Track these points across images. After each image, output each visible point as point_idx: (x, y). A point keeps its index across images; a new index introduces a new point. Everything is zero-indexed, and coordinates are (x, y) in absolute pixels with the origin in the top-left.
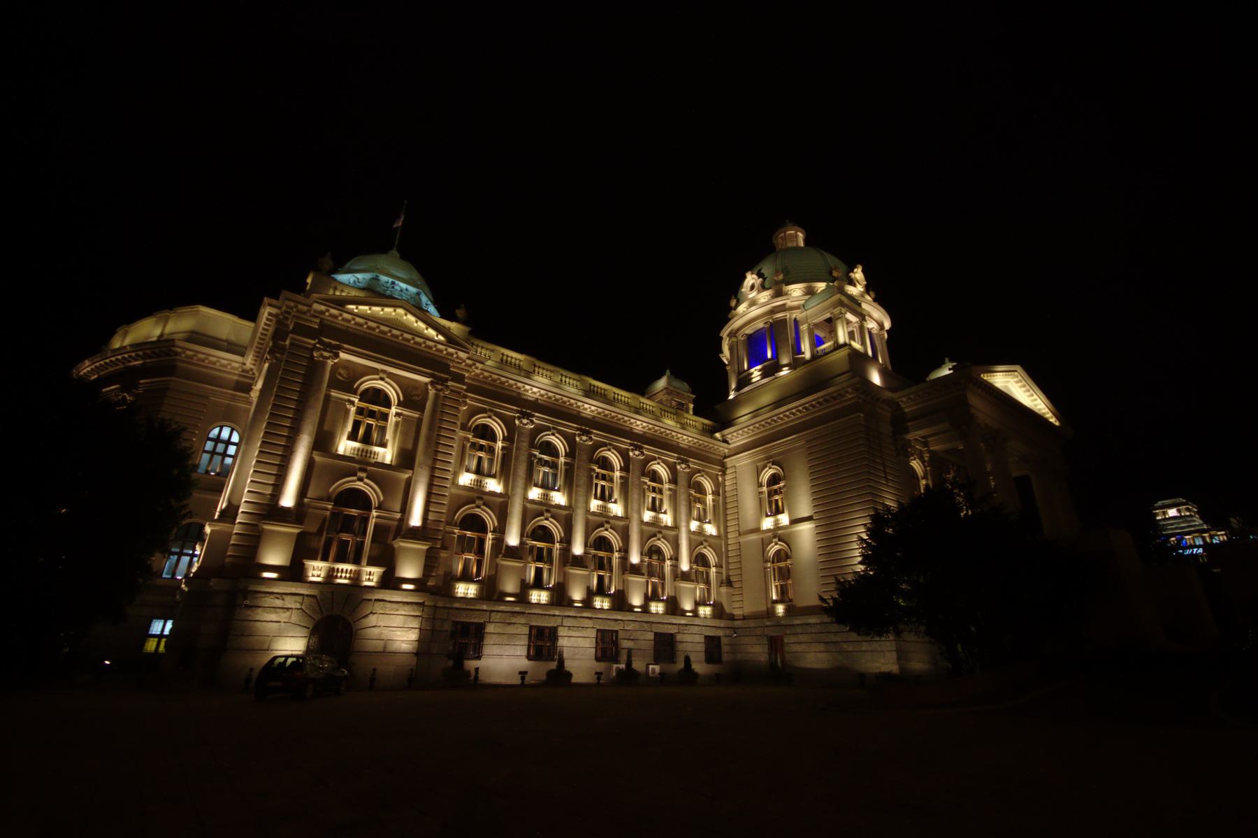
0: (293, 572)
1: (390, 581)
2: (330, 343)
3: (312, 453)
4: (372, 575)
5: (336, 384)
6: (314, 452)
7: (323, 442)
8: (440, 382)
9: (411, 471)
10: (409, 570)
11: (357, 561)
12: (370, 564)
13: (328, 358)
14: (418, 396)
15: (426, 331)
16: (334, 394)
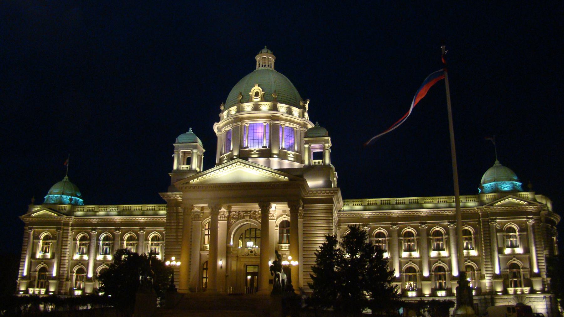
0: (505, 292)
1: (533, 291)
2: (493, 218)
3: (498, 255)
4: (527, 290)
5: (498, 231)
6: (499, 255)
7: (500, 251)
8: (530, 219)
9: (529, 254)
10: (538, 287)
11: (521, 286)
12: (525, 286)
13: (494, 224)
14: (524, 226)
15: (520, 203)
16: (498, 234)
